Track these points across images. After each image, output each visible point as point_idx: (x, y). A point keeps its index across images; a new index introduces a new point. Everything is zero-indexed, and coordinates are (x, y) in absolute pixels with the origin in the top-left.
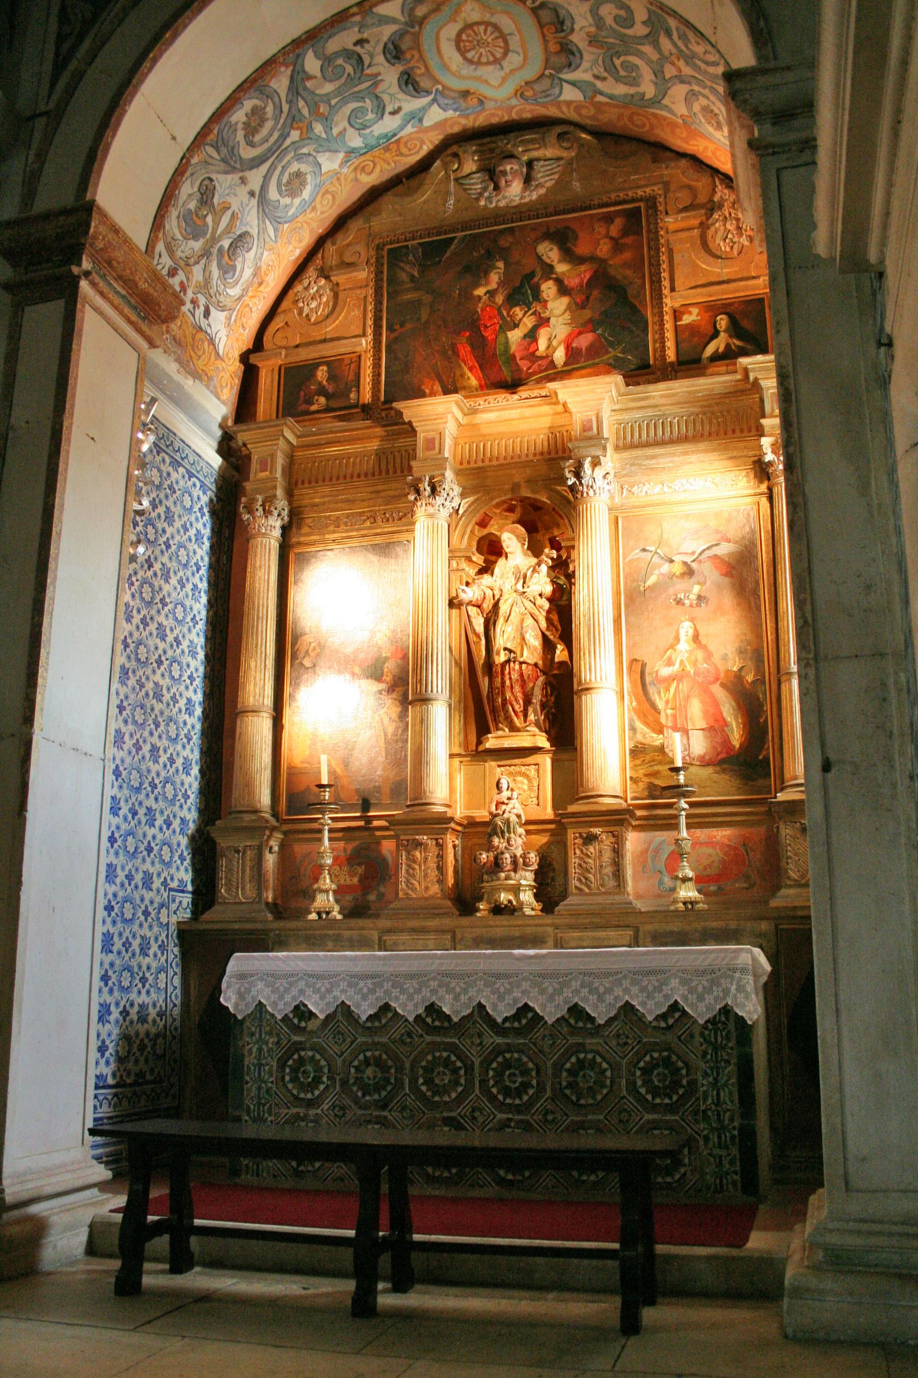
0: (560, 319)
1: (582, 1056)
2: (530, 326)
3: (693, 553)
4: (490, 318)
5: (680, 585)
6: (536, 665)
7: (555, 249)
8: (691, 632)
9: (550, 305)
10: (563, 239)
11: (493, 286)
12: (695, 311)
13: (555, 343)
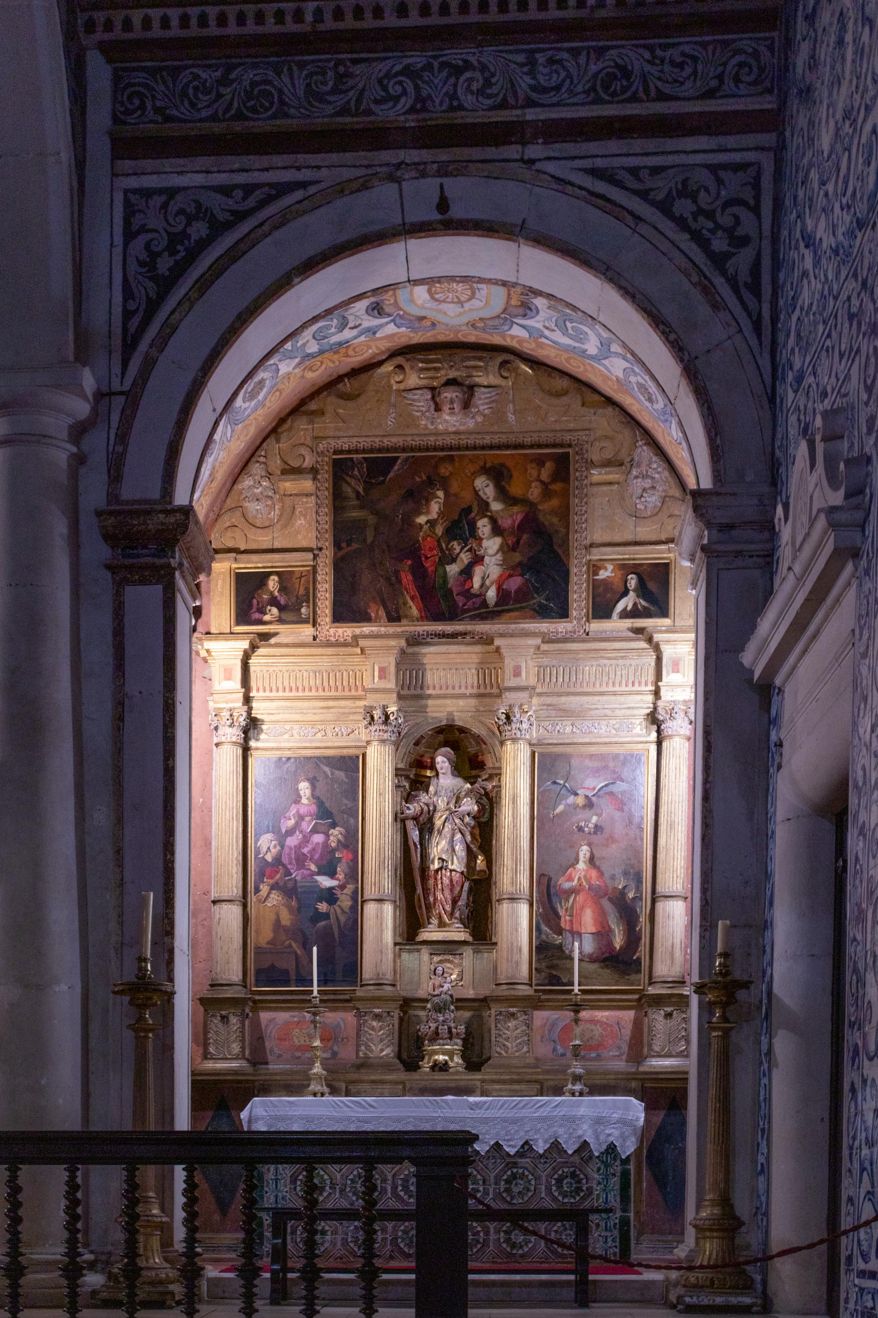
0: (493, 559)
1: (515, 1170)
2: (466, 562)
3: (594, 789)
4: (431, 549)
5: (582, 815)
6: (462, 873)
7: (491, 486)
8: (588, 855)
9: (485, 543)
10: (499, 475)
11: (434, 515)
12: (610, 567)
13: (487, 582)
